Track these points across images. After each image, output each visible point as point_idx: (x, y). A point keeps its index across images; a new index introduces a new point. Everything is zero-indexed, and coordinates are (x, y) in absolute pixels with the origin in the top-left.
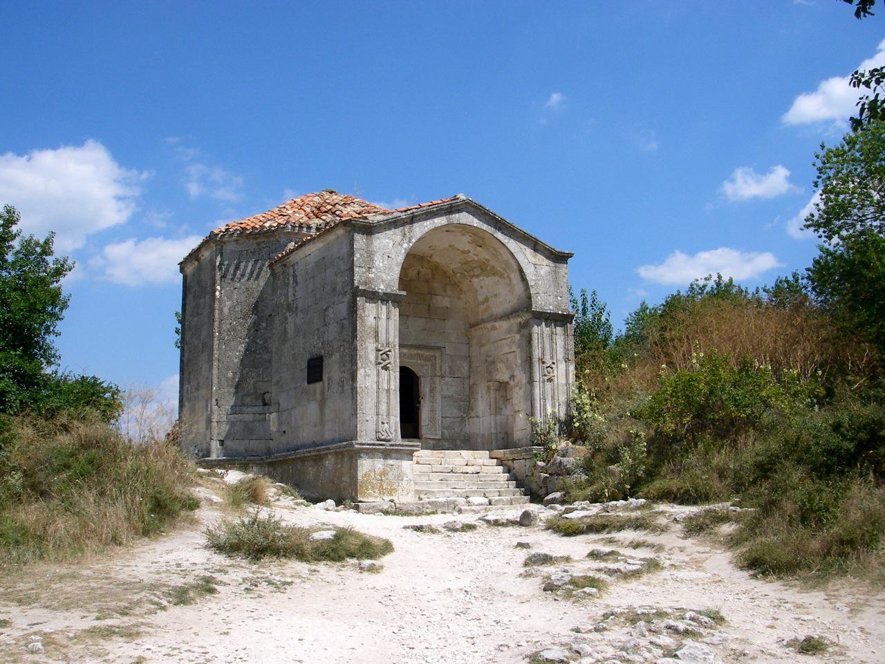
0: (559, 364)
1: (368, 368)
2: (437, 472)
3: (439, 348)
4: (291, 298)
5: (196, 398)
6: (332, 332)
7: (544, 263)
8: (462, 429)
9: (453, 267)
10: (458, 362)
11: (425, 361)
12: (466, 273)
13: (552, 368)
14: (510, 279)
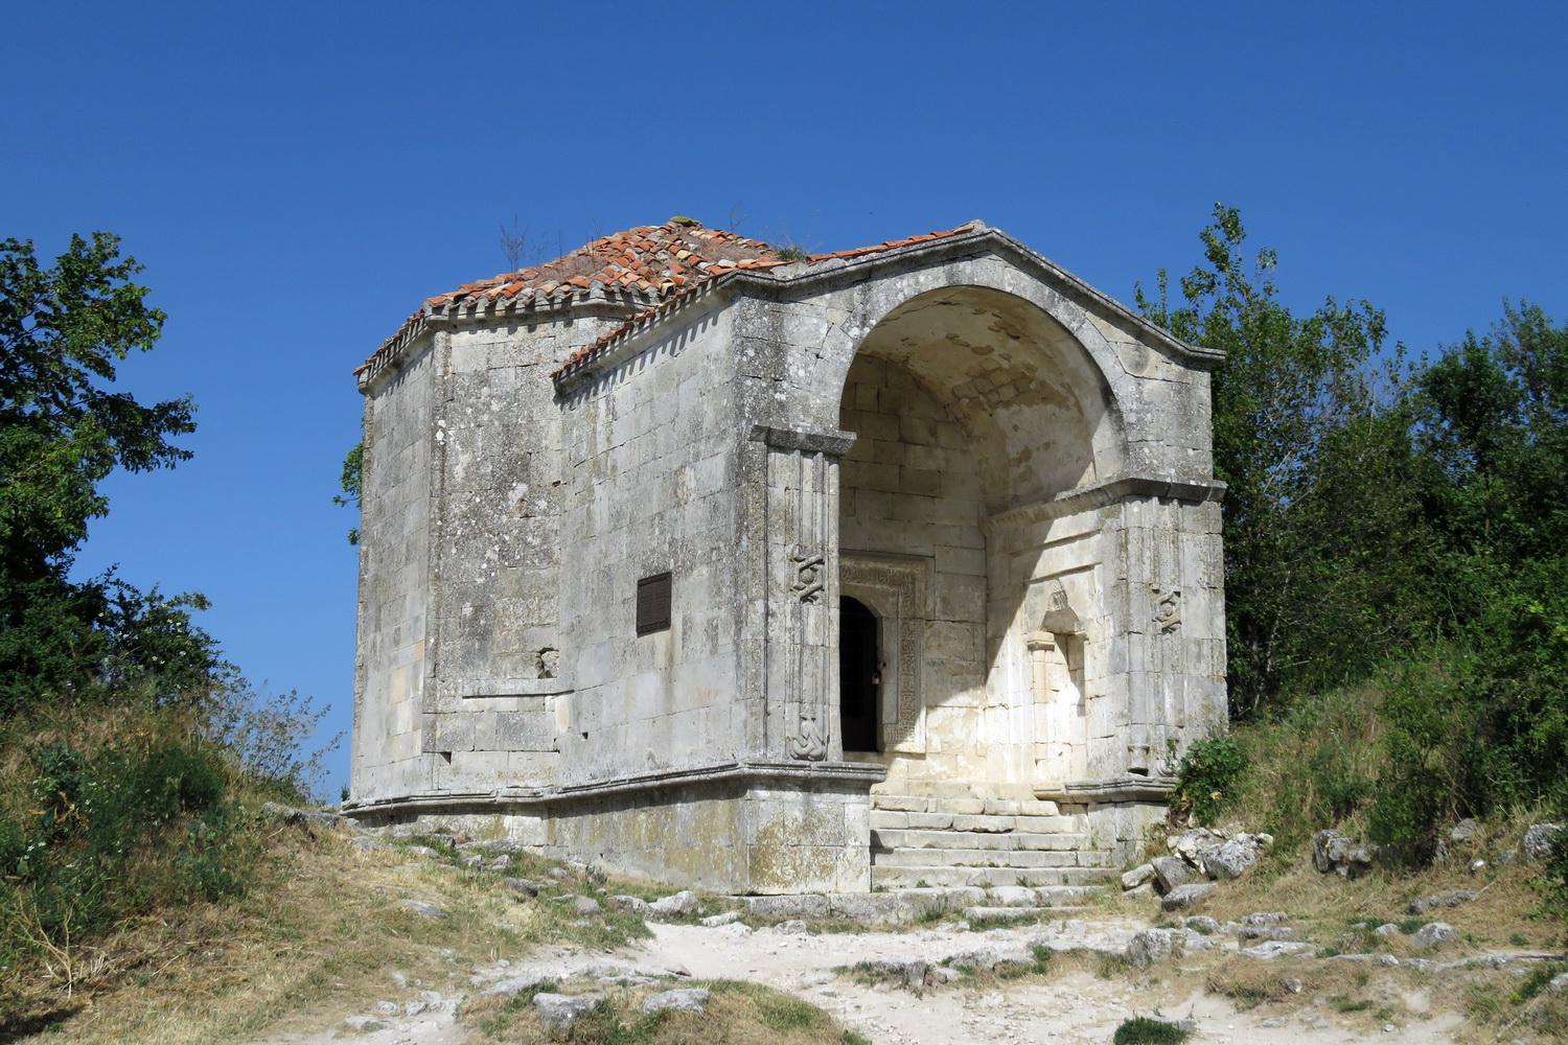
0: (1189, 597)
1: (771, 600)
2: (917, 828)
3: (919, 558)
4: (601, 447)
5: (393, 660)
6: (692, 519)
7: (1160, 375)
8: (968, 735)
9: (953, 383)
11: (892, 584)
12: (982, 398)
13: (1173, 604)
14: (1080, 411)
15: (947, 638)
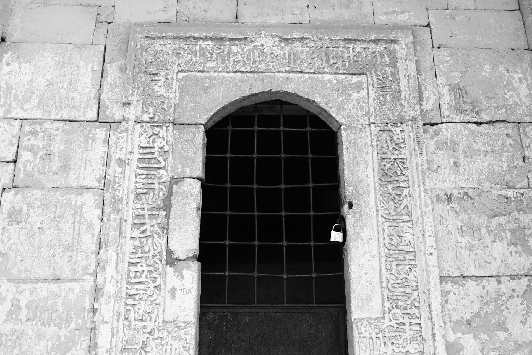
10: (487, 67)
15: (470, 153)
